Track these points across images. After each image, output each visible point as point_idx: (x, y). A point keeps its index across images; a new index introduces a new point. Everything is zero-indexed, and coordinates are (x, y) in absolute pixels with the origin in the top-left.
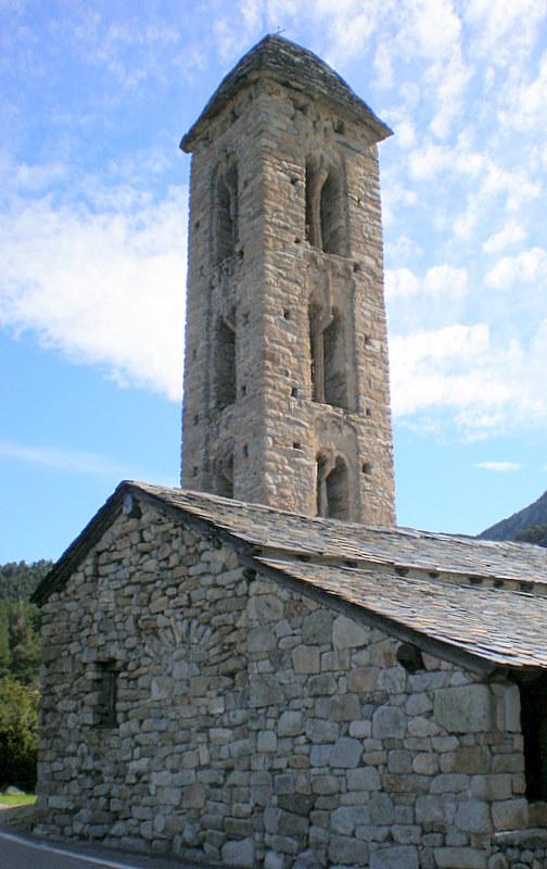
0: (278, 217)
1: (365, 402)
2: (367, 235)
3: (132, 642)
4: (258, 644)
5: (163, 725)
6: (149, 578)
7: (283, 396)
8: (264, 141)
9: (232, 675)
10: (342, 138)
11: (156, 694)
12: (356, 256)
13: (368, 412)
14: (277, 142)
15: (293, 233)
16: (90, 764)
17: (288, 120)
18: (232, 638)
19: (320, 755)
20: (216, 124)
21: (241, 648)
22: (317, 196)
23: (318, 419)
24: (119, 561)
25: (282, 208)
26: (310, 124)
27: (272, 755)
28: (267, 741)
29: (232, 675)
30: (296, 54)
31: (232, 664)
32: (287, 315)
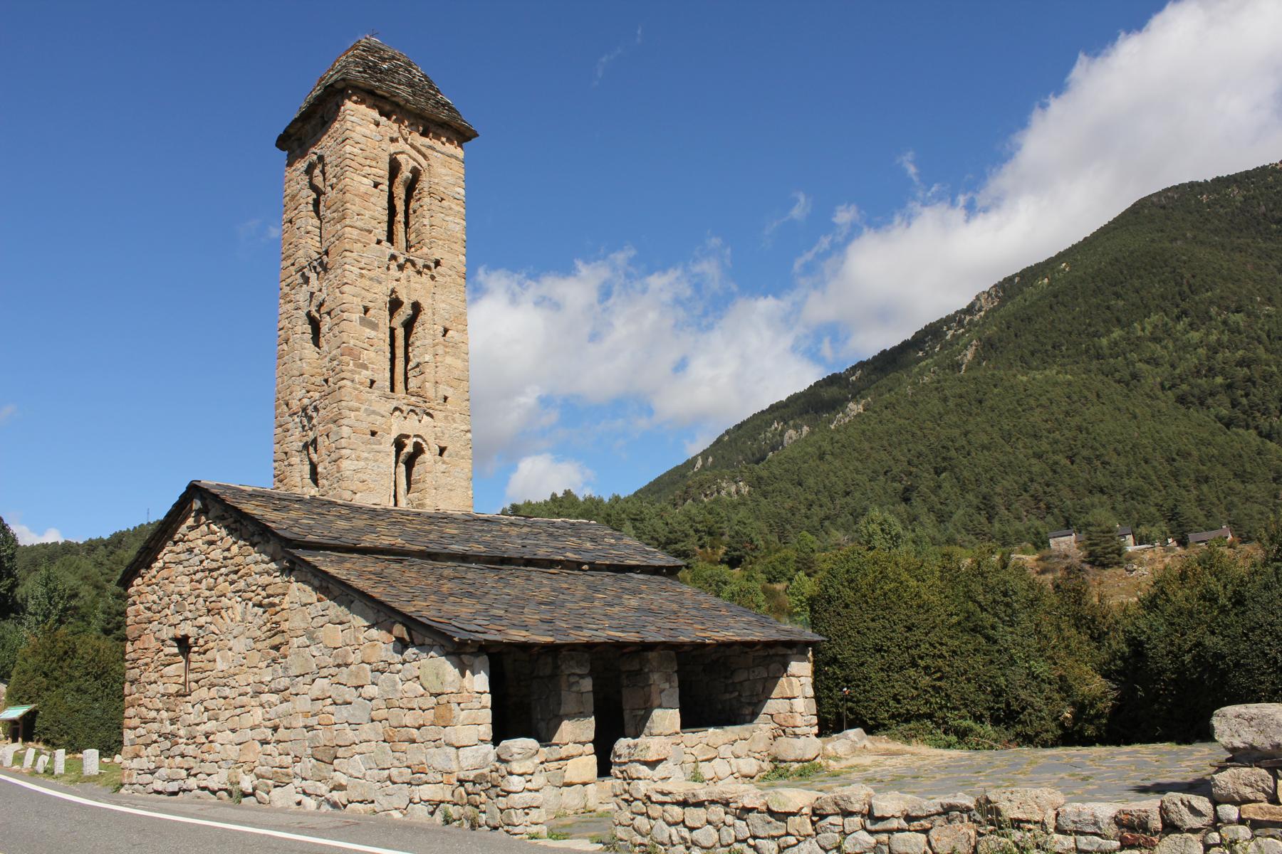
3: (202, 621)
4: (296, 622)
5: (227, 691)
6: (215, 565)
8: (348, 149)
9: (276, 648)
10: (426, 141)
11: (220, 665)
13: (446, 399)
16: (168, 728)
17: (373, 126)
18: (276, 618)
19: (344, 712)
20: (308, 127)
21: (285, 626)
22: (400, 192)
23: (396, 409)
24: (190, 550)
27: (306, 714)
28: (303, 704)
29: (276, 648)
30: (384, 60)
31: (277, 640)
32: (366, 310)
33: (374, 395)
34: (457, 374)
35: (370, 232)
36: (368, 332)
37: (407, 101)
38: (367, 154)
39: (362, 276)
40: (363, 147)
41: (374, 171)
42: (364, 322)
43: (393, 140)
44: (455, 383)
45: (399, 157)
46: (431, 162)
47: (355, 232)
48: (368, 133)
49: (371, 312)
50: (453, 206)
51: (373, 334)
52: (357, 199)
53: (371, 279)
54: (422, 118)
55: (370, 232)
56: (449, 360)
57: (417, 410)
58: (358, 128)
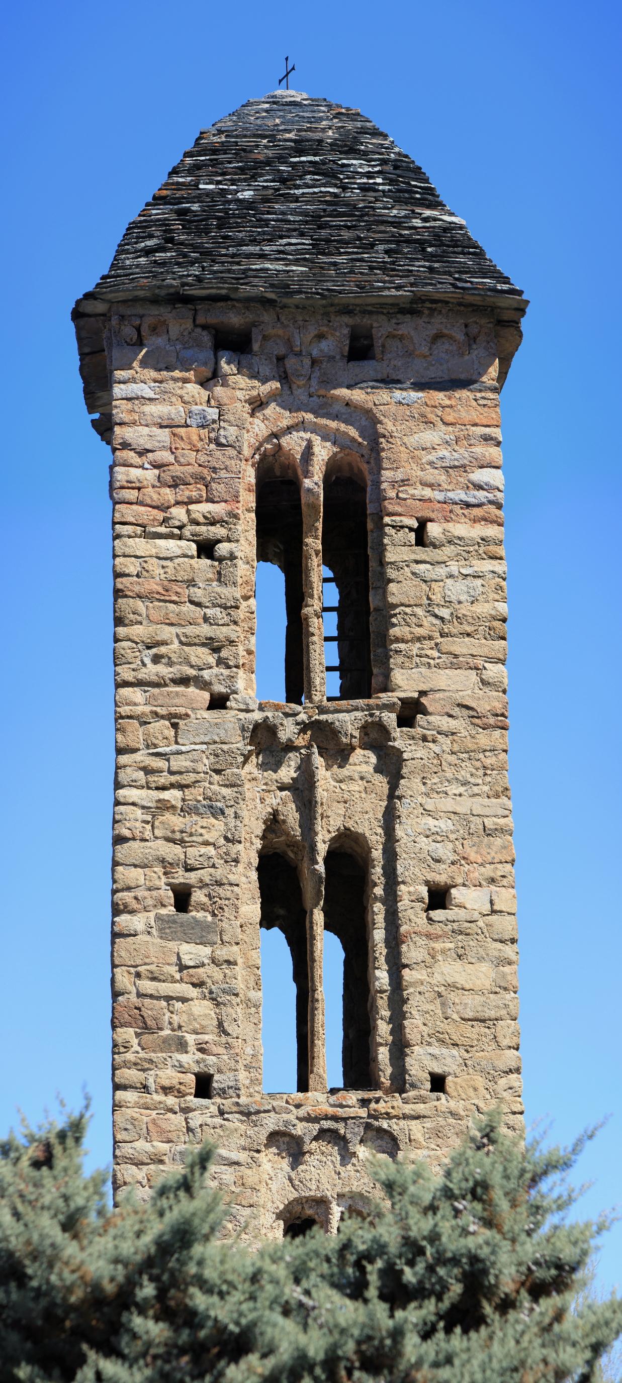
0: (156, 659)
1: (420, 1062)
2: (445, 613)
7: (171, 1101)
12: (406, 681)
13: (438, 1083)
14: (155, 467)
15: (204, 685)
17: (193, 389)
23: (274, 1137)
25: (167, 633)
26: (265, 370)
30: (251, 171)
33: (204, 1112)
34: (471, 1005)
35: (184, 681)
36: (191, 952)
37: (283, 287)
38: (177, 470)
39: (164, 806)
40: (165, 456)
41: (201, 509)
42: (166, 929)
43: (257, 405)
44: (474, 1032)
45: (285, 441)
46: (388, 425)
47: (135, 694)
48: (176, 411)
49: (199, 896)
50: (461, 529)
51: (207, 950)
52: (140, 605)
53: (187, 810)
54: (347, 310)
55: (184, 681)
56: (450, 970)
57: (341, 1128)
58: (149, 409)
